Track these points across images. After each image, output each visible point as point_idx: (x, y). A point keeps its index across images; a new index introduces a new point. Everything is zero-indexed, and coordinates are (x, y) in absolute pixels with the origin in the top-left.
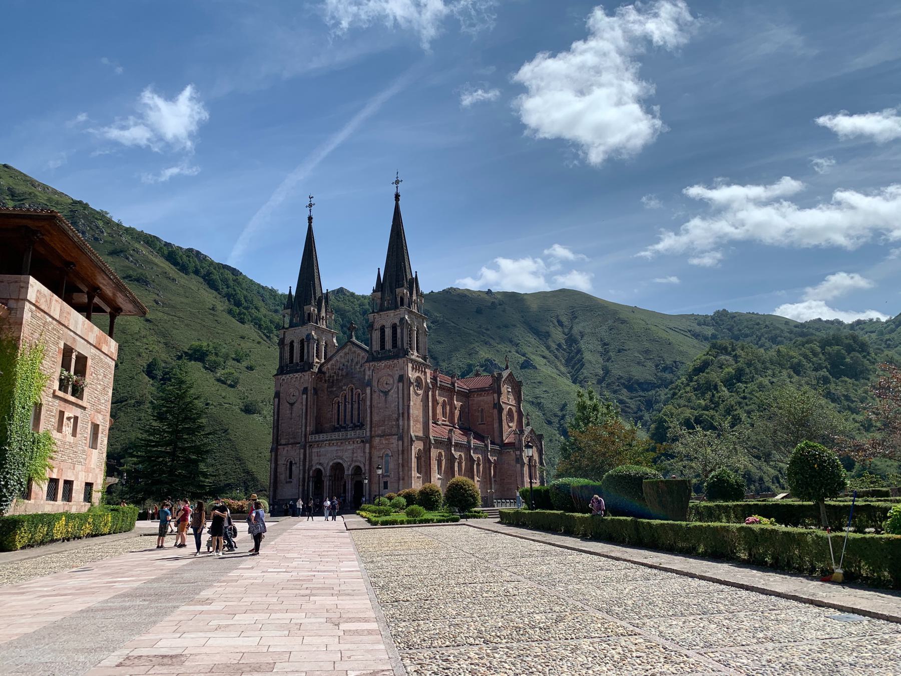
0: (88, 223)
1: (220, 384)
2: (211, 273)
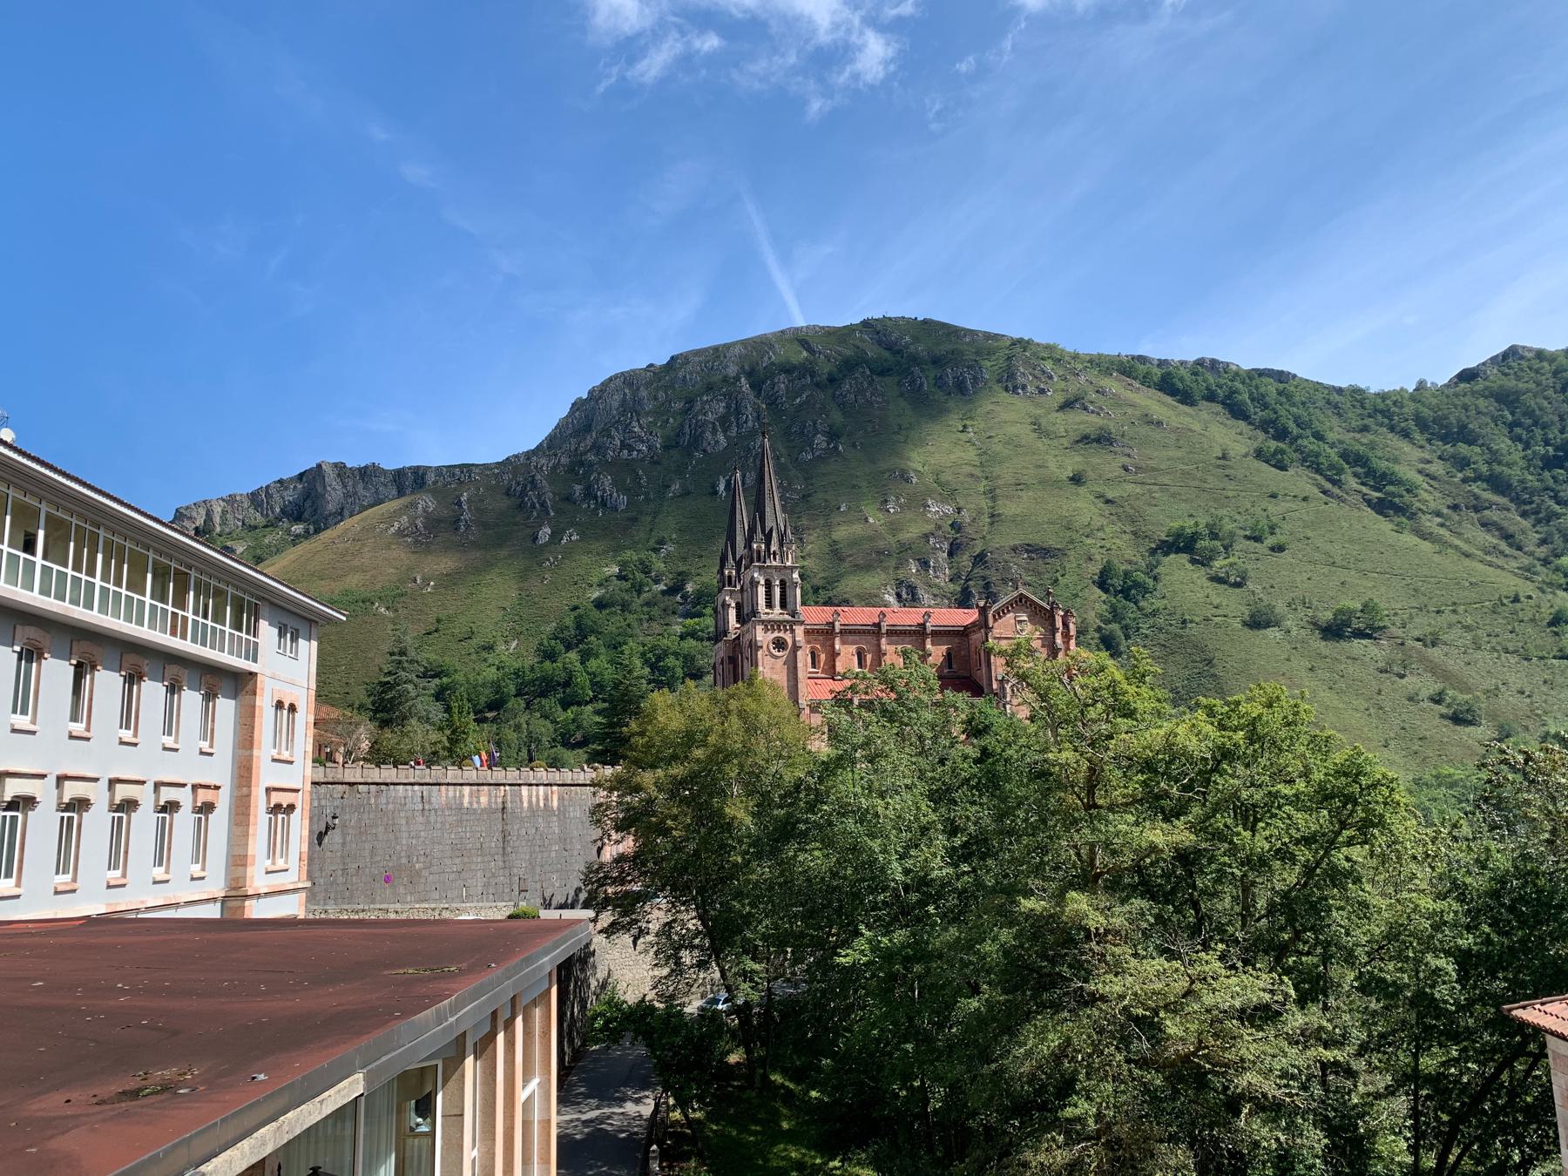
0: (1031, 370)
1: (1215, 585)
2: (1235, 392)
